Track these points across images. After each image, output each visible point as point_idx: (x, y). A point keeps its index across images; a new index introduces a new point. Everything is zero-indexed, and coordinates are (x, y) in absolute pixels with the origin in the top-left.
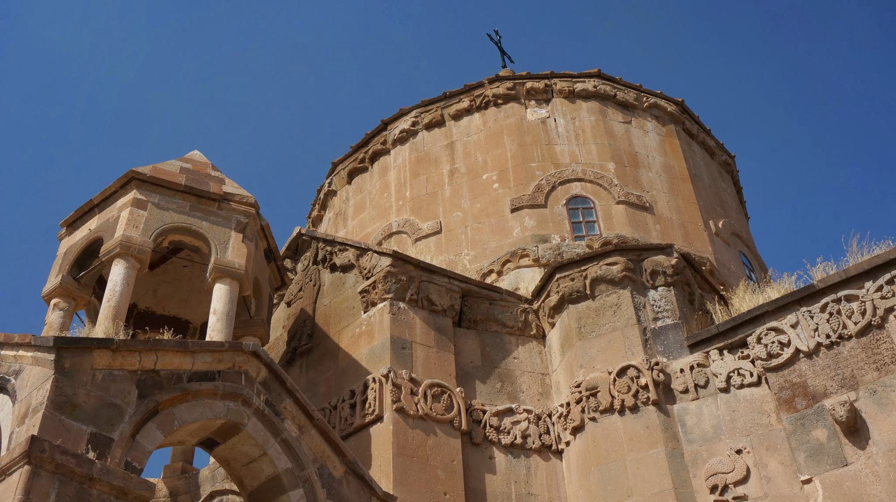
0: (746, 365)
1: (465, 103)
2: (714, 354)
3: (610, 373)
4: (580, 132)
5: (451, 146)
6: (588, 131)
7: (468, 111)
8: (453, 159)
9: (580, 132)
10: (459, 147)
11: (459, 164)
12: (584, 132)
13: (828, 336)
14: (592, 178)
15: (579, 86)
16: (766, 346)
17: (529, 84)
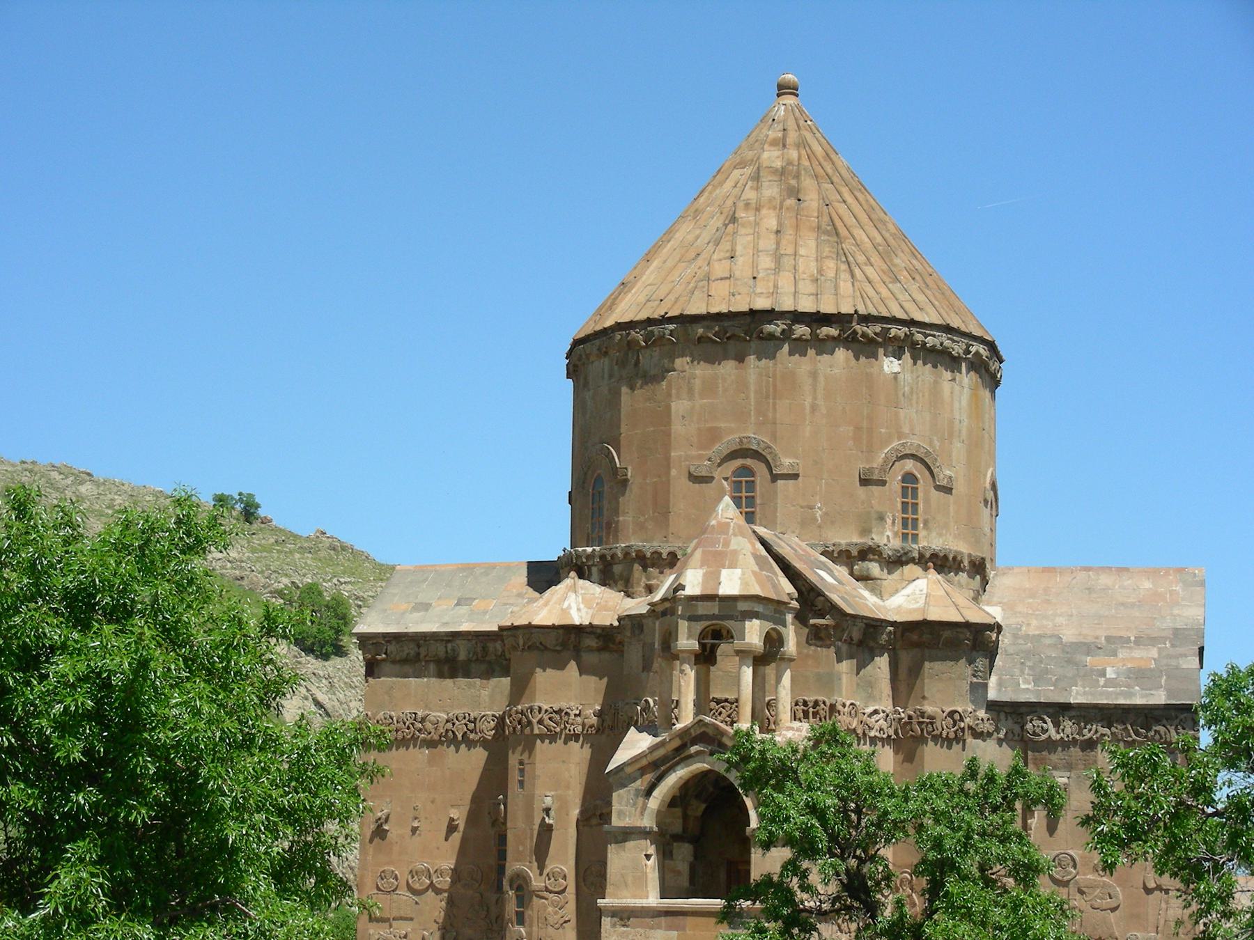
0: (1017, 729)
1: (833, 331)
2: (1002, 716)
3: (943, 712)
4: (921, 395)
5: (814, 375)
6: (927, 394)
7: (836, 341)
8: (815, 391)
9: (921, 395)
10: (821, 379)
11: (820, 402)
12: (923, 396)
13: (1068, 736)
14: (922, 456)
15: (930, 341)
16: (1034, 726)
17: (893, 332)
